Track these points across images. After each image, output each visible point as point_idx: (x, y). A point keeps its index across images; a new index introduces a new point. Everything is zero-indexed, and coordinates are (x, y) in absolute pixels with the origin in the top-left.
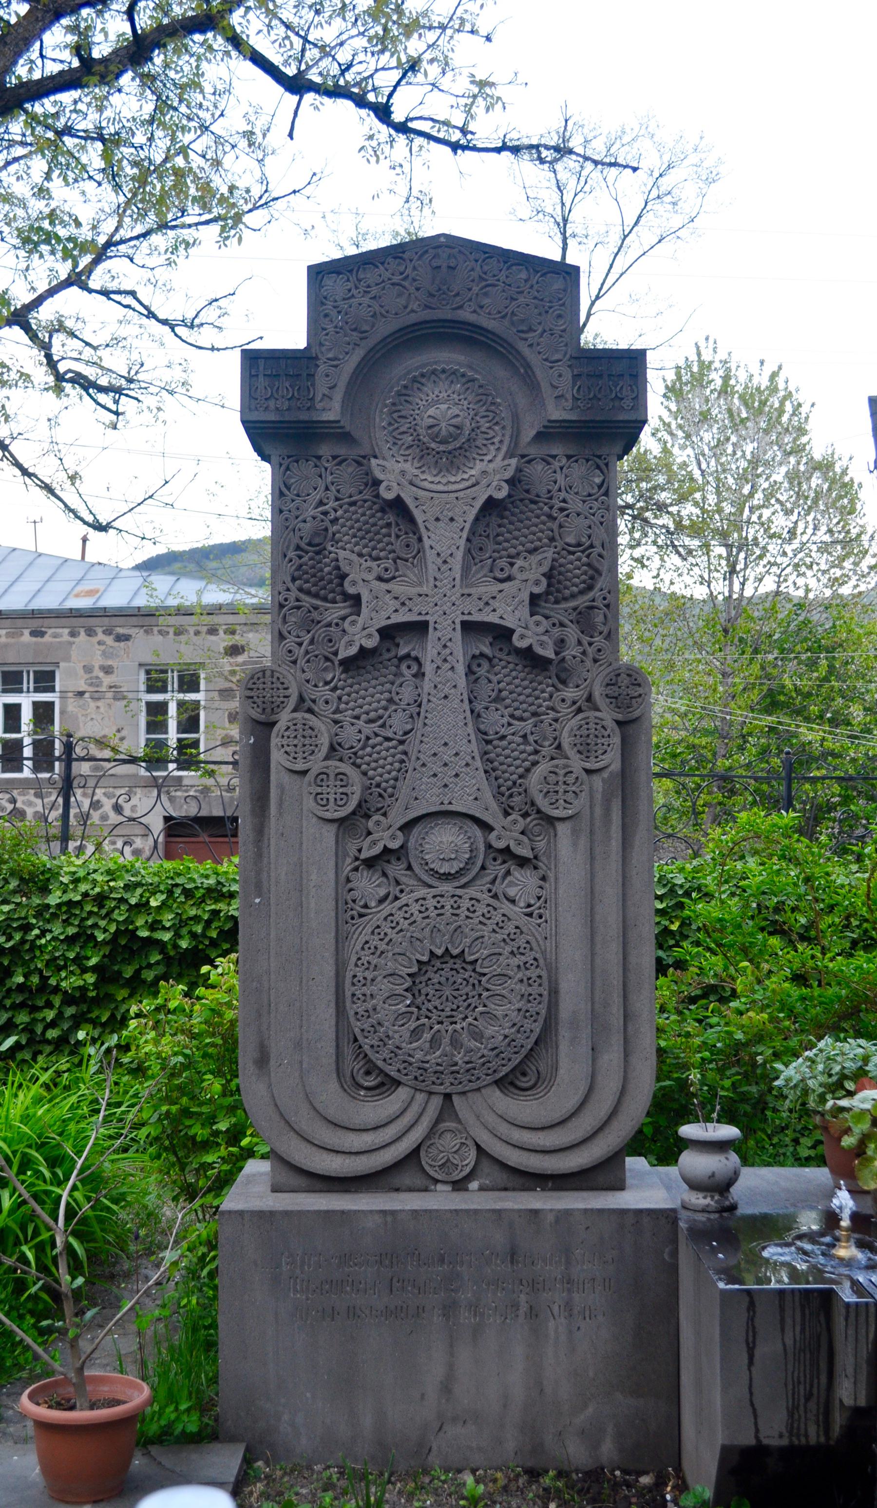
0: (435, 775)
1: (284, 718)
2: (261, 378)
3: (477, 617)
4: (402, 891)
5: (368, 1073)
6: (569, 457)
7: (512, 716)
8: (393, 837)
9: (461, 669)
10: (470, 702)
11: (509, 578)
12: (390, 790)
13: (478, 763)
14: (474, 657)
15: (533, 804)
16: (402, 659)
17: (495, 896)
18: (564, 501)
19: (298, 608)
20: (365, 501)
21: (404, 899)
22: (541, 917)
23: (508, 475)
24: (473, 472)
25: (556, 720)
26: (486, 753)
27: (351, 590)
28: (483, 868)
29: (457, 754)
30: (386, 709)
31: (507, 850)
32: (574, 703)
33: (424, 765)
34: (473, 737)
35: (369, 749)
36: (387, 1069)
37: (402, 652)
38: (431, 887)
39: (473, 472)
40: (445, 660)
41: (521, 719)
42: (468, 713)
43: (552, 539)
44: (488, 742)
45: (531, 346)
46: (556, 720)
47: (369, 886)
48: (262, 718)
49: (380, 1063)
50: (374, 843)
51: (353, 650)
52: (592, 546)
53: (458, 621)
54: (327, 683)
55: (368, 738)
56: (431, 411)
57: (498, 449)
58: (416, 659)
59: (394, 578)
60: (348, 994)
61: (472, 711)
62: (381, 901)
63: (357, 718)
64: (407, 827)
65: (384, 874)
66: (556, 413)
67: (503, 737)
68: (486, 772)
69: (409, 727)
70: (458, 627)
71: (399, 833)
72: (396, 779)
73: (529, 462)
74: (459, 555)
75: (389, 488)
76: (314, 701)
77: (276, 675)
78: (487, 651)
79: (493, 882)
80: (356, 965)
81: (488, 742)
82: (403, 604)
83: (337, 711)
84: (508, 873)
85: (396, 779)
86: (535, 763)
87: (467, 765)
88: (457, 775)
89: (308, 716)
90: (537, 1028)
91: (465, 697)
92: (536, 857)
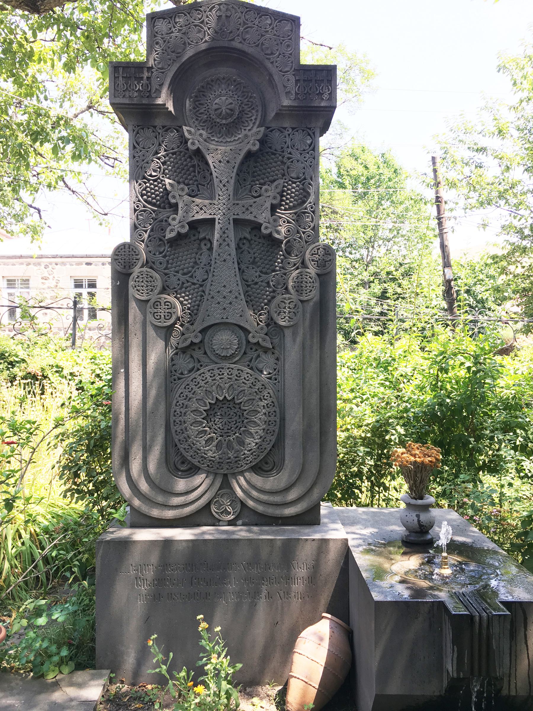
0: (219, 303)
1: (136, 270)
2: (121, 78)
3: (241, 216)
4: (201, 366)
5: (183, 463)
6: (293, 129)
7: (261, 272)
8: (196, 337)
9: (233, 245)
10: (239, 264)
11: (260, 196)
12: (195, 311)
13: (242, 296)
14: (241, 239)
15: (272, 319)
16: (201, 240)
17: (251, 369)
18: (290, 153)
19: (145, 211)
20: (181, 152)
21: (202, 371)
22: (276, 380)
23: (259, 137)
24: (240, 136)
25: (285, 274)
26: (247, 292)
27: (173, 201)
28: (245, 353)
29: (230, 292)
30: (193, 267)
31: (258, 343)
32: (295, 265)
33: (213, 297)
34: (239, 283)
35: (184, 289)
36: (193, 461)
37: (202, 236)
38: (216, 363)
39: (240, 136)
40: (224, 240)
41: (266, 273)
42: (237, 269)
43: (283, 175)
44: (248, 286)
45: (272, 63)
46: (285, 274)
47: (185, 363)
48: (124, 271)
49: (189, 458)
50: (186, 339)
51: (173, 234)
52: (305, 179)
53: (231, 219)
54: (160, 253)
55: (183, 283)
56: (217, 101)
57: (254, 123)
58: (209, 240)
59: (197, 195)
60: (172, 421)
61: (239, 269)
62: (190, 371)
63: (177, 272)
64: (203, 331)
65: (192, 357)
66: (286, 102)
67: (256, 283)
68: (247, 302)
69: (206, 277)
70: (232, 222)
71: (199, 334)
72: (199, 306)
73: (271, 131)
74: (232, 181)
75: (193, 143)
76: (154, 263)
77: (131, 247)
78: (248, 236)
79: (250, 361)
80: (176, 405)
81: (248, 286)
82: (201, 209)
83: (166, 268)
84: (259, 356)
85: (199, 306)
86: (273, 297)
87: (236, 297)
88: (230, 303)
89: (149, 270)
90: (274, 439)
91: (235, 260)
92: (273, 348)
